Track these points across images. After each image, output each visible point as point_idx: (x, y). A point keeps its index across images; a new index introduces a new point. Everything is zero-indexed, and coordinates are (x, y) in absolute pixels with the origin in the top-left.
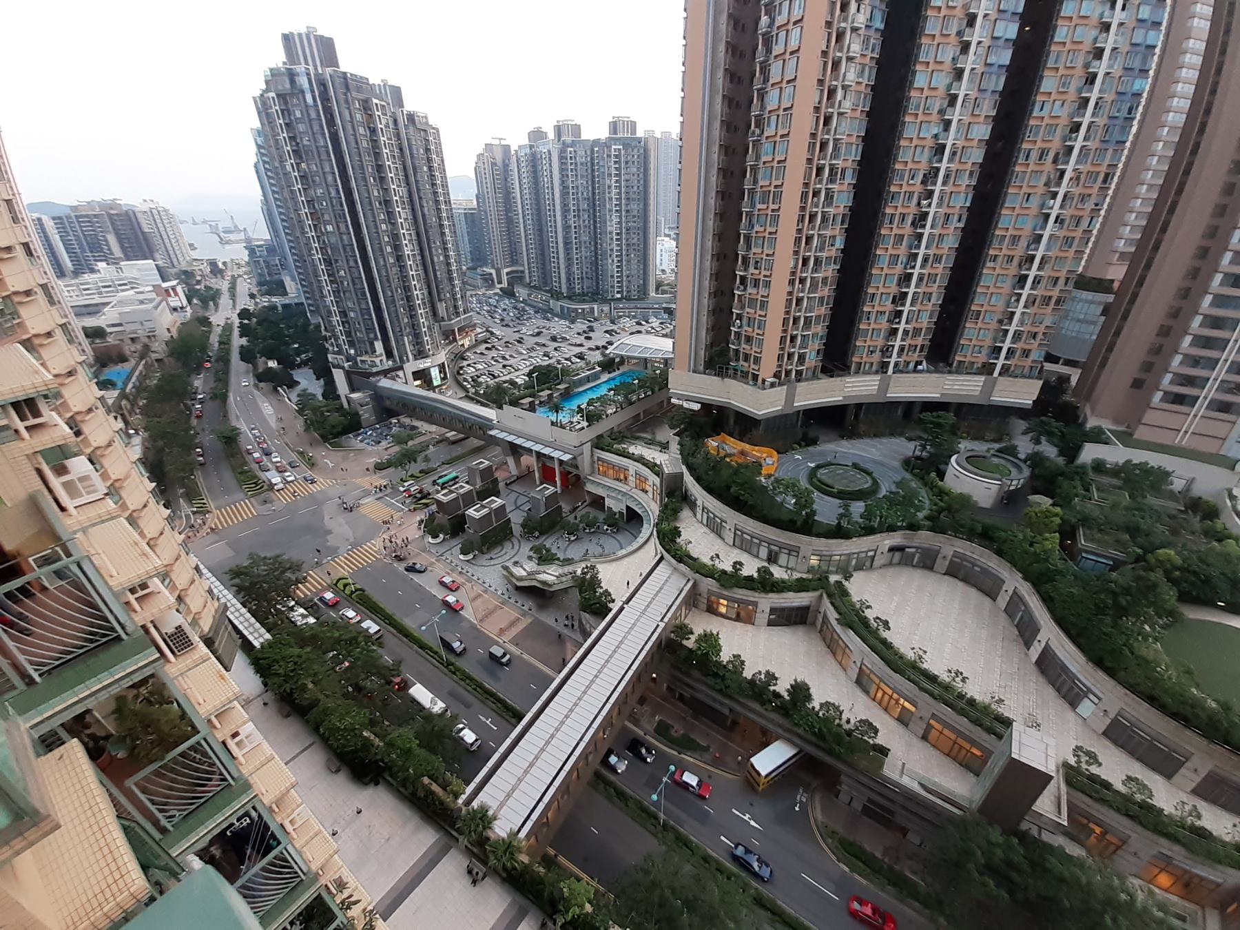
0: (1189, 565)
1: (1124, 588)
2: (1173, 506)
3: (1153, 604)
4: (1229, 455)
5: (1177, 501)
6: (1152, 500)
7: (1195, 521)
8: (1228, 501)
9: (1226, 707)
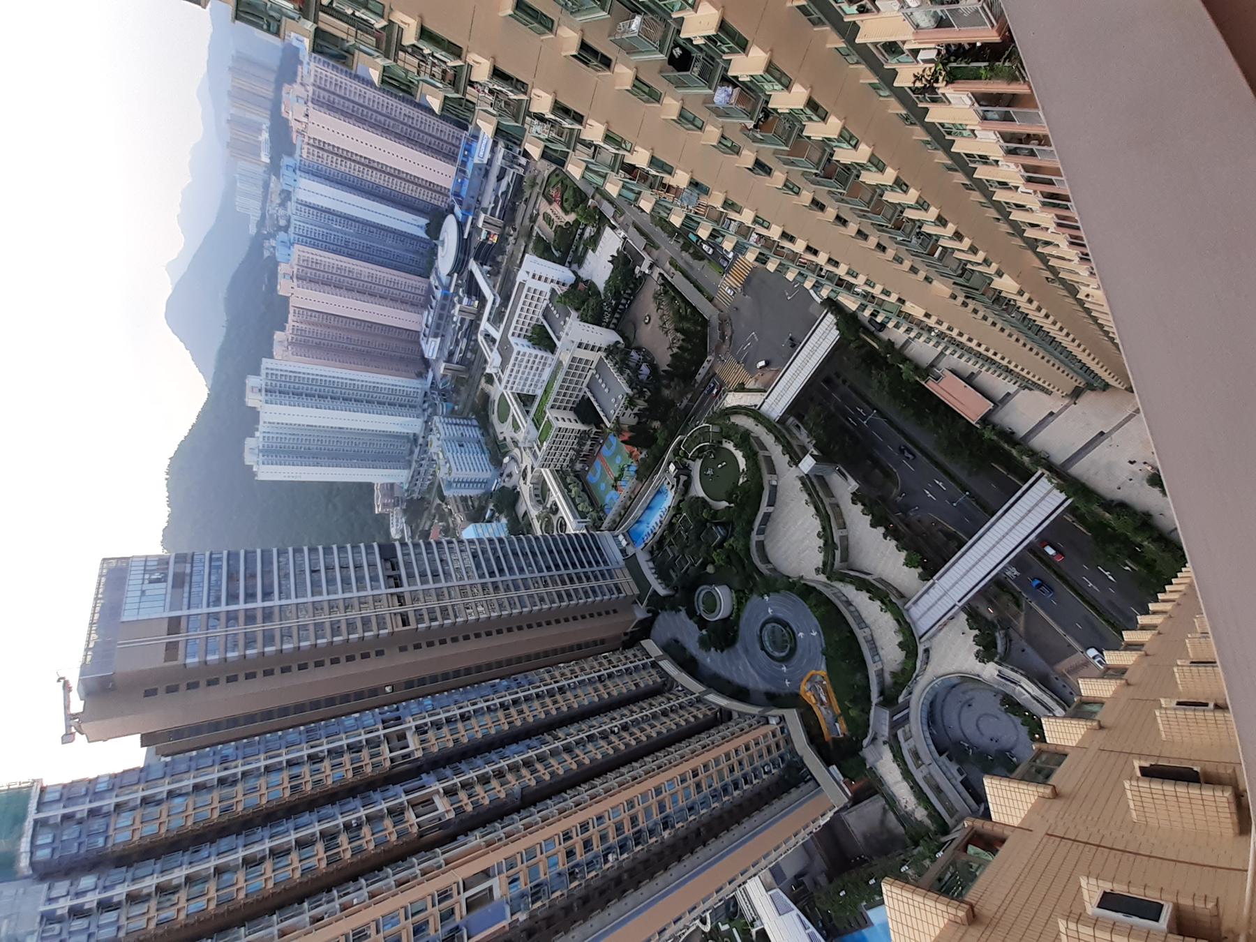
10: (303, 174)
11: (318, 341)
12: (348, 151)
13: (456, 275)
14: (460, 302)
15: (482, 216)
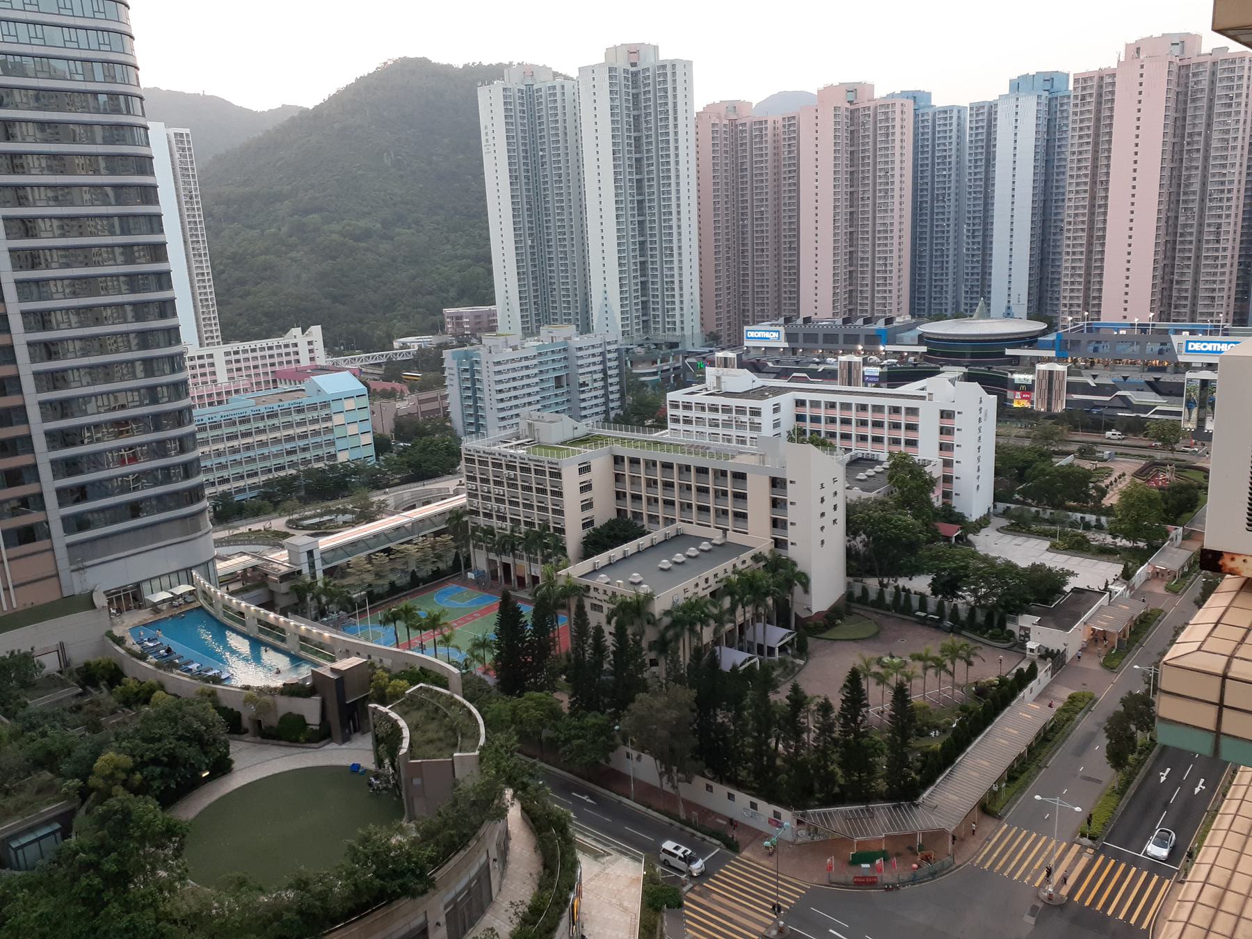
0: (142, 757)
1: (94, 849)
2: (69, 692)
3: (143, 839)
4: (77, 591)
5: (64, 684)
6: (37, 703)
7: (103, 695)
8: (117, 648)
9: (301, 885)
10: (1044, 101)
11: (748, 166)
12: (1110, 142)
13: (924, 349)
14: (865, 363)
15: (1060, 368)
